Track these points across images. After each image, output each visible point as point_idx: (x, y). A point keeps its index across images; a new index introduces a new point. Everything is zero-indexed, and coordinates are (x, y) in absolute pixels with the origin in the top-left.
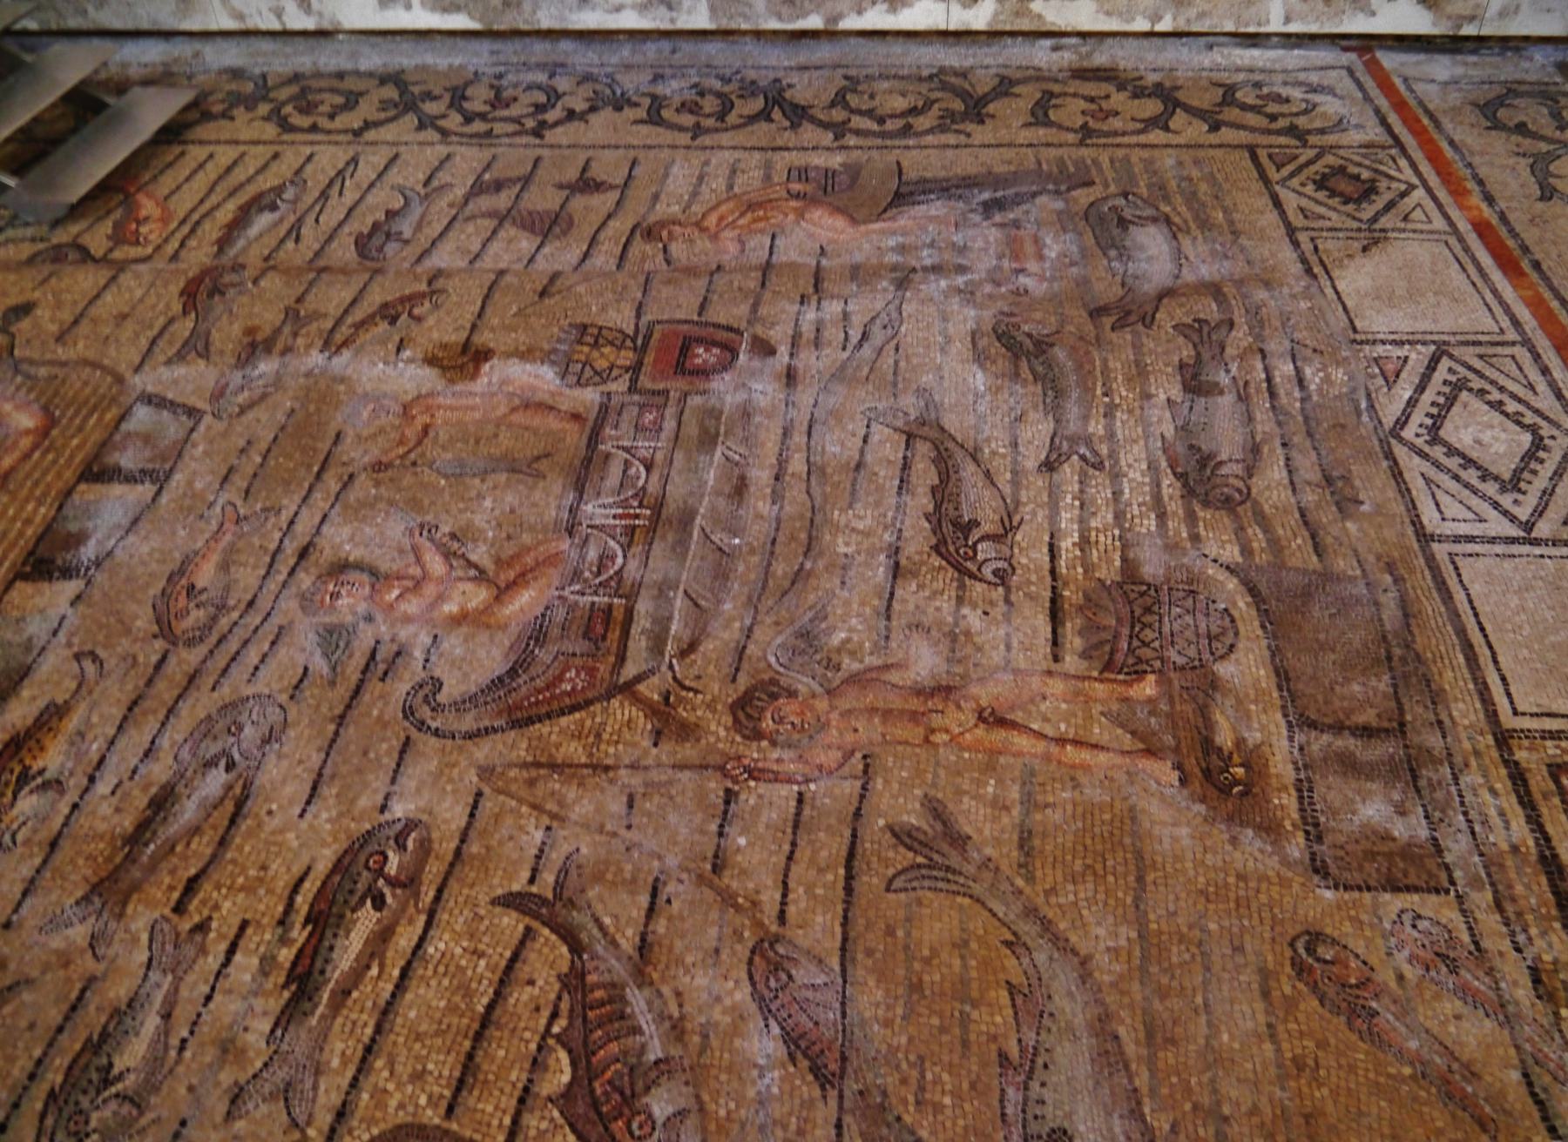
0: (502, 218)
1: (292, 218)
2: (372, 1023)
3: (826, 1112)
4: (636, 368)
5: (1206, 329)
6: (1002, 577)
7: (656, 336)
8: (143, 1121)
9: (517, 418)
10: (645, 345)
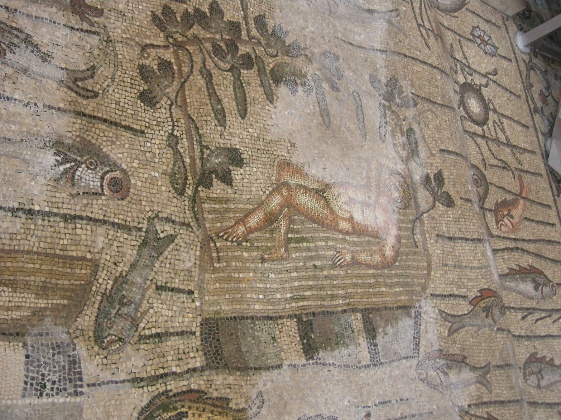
1: (533, 304)
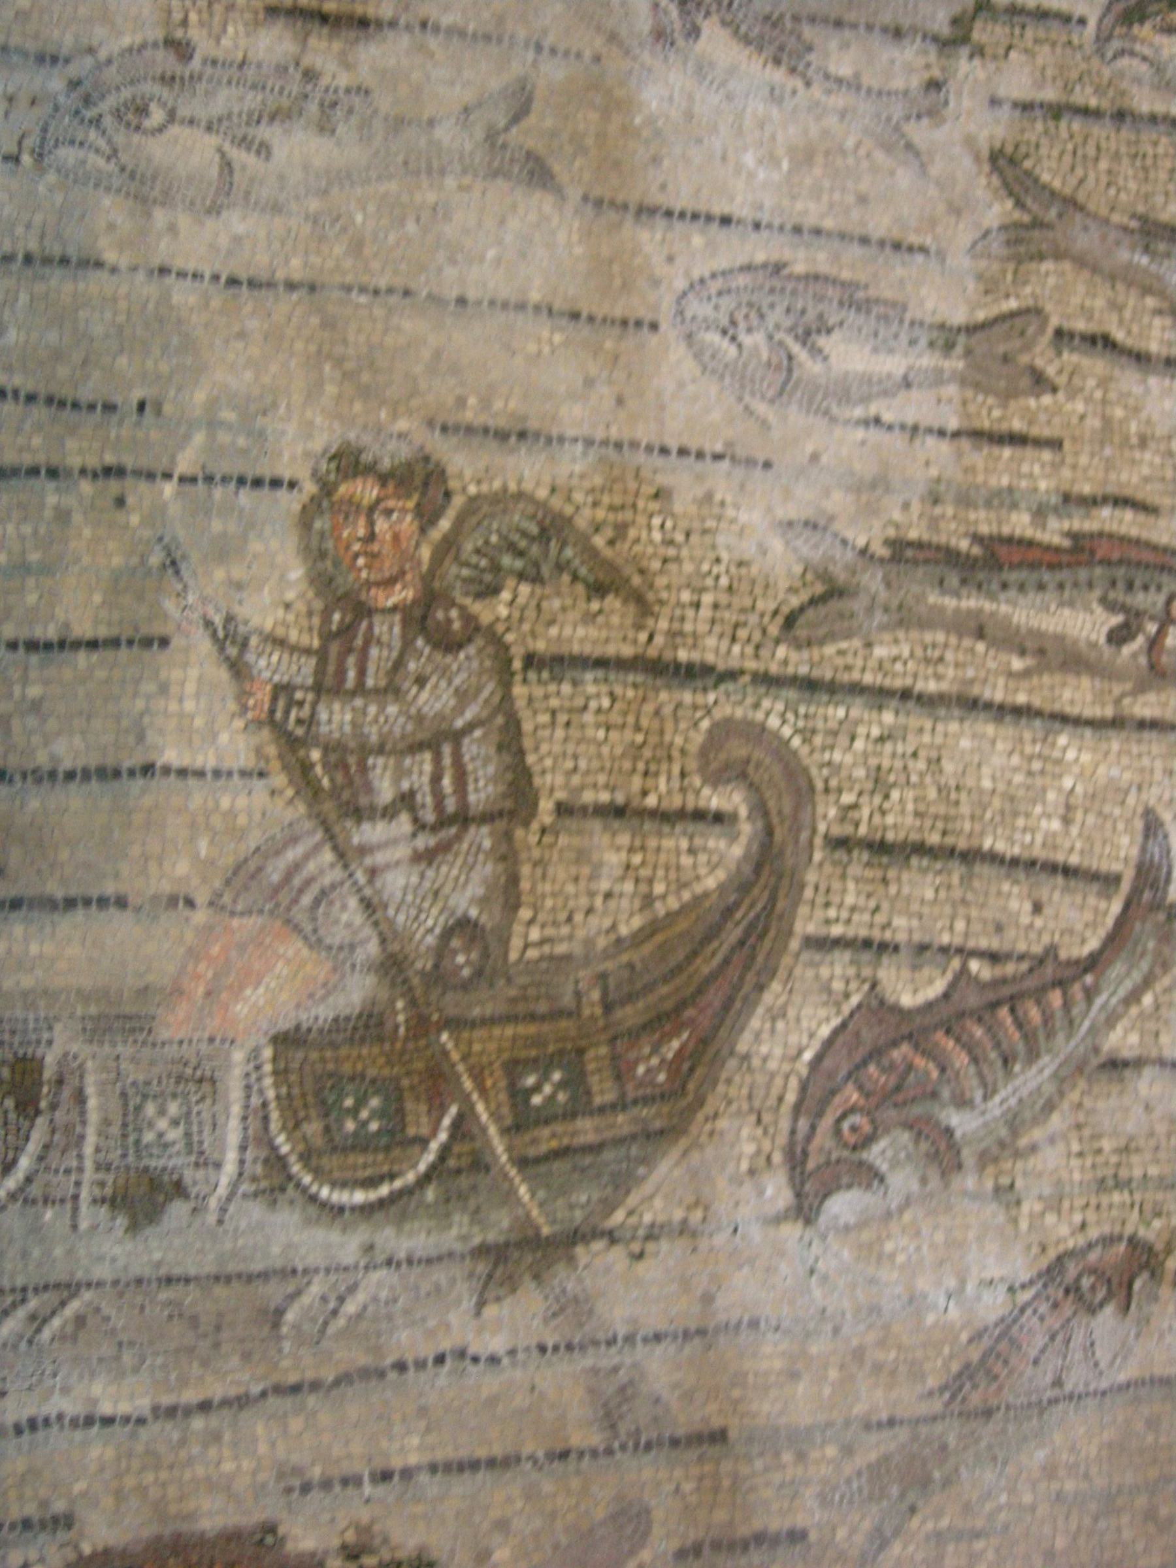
2: (944, 686)
8: (761, 408)
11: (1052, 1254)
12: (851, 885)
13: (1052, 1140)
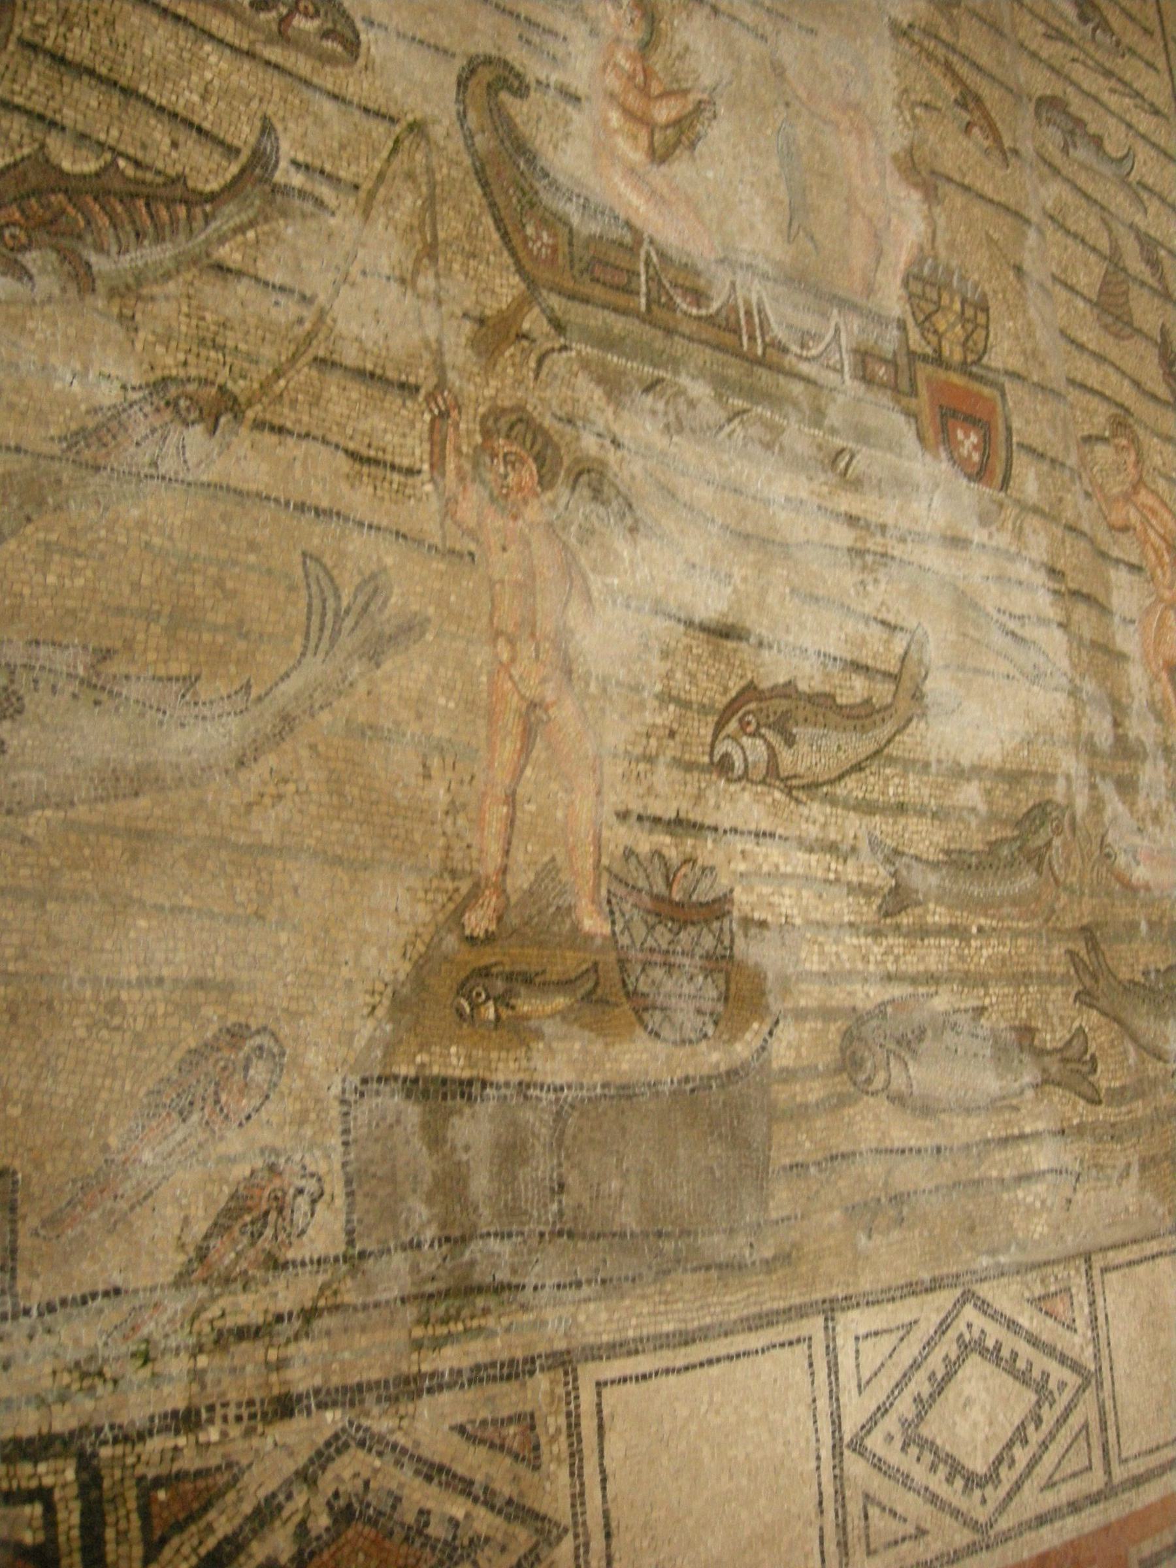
0: (1114, 259)
3: (34, 437)
4: (939, 360)
5: (1085, 1069)
6: (723, 766)
7: (987, 391)
9: (859, 224)
10: (972, 376)
11: (159, 373)
12: (34, 75)
13: (167, 298)
